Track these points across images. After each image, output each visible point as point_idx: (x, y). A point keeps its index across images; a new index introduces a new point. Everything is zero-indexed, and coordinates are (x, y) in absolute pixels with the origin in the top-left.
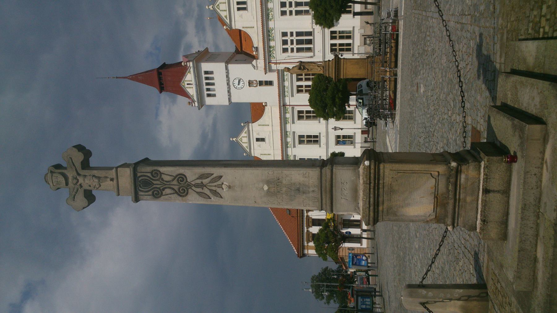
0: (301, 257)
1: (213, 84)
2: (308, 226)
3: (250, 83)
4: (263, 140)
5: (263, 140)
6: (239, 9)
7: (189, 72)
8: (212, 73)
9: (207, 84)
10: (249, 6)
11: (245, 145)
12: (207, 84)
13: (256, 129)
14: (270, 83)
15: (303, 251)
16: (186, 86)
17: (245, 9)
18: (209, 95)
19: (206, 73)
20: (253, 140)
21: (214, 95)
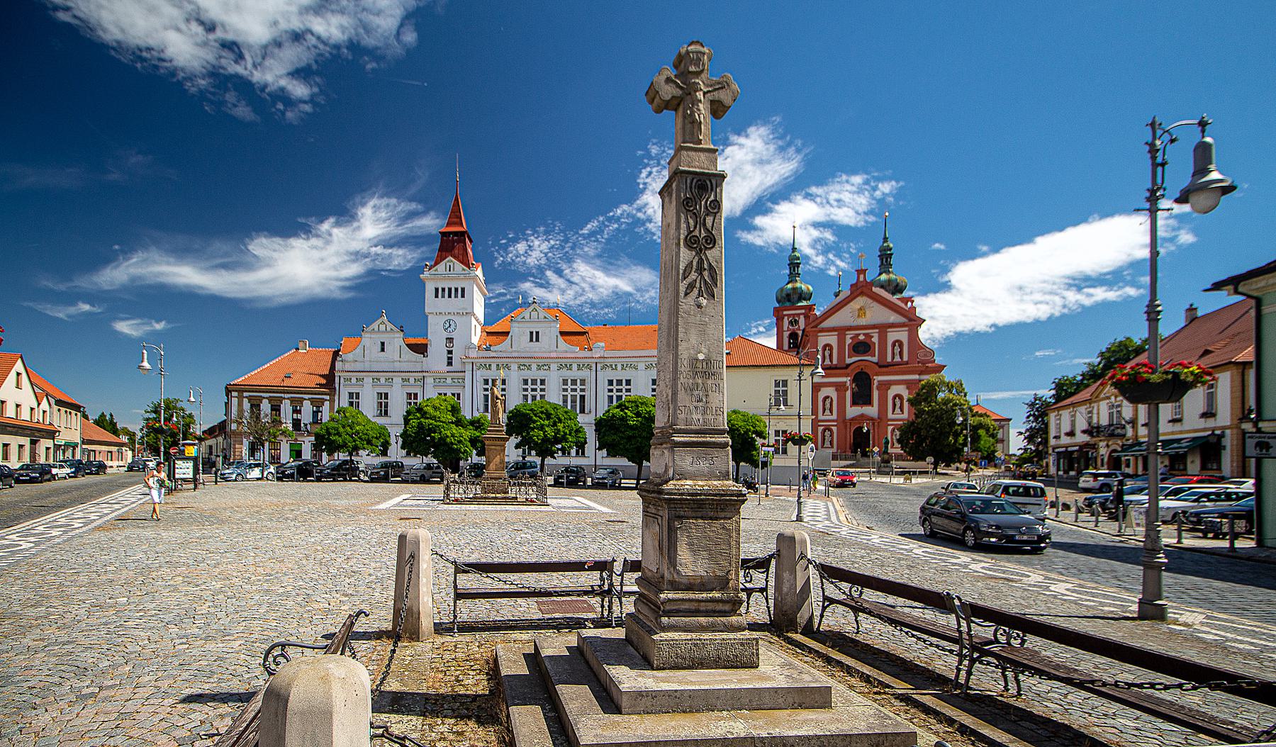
0: (226, 388)
1: (450, 296)
2: (270, 399)
3: (450, 340)
4: (383, 350)
5: (383, 350)
6: (531, 333)
7: (464, 270)
8: (463, 296)
9: (450, 290)
10: (534, 344)
11: (375, 326)
12: (450, 290)
13: (396, 341)
14: (450, 364)
15: (236, 391)
16: (448, 264)
17: (531, 340)
18: (437, 290)
19: (463, 290)
20: (384, 338)
21: (437, 296)
